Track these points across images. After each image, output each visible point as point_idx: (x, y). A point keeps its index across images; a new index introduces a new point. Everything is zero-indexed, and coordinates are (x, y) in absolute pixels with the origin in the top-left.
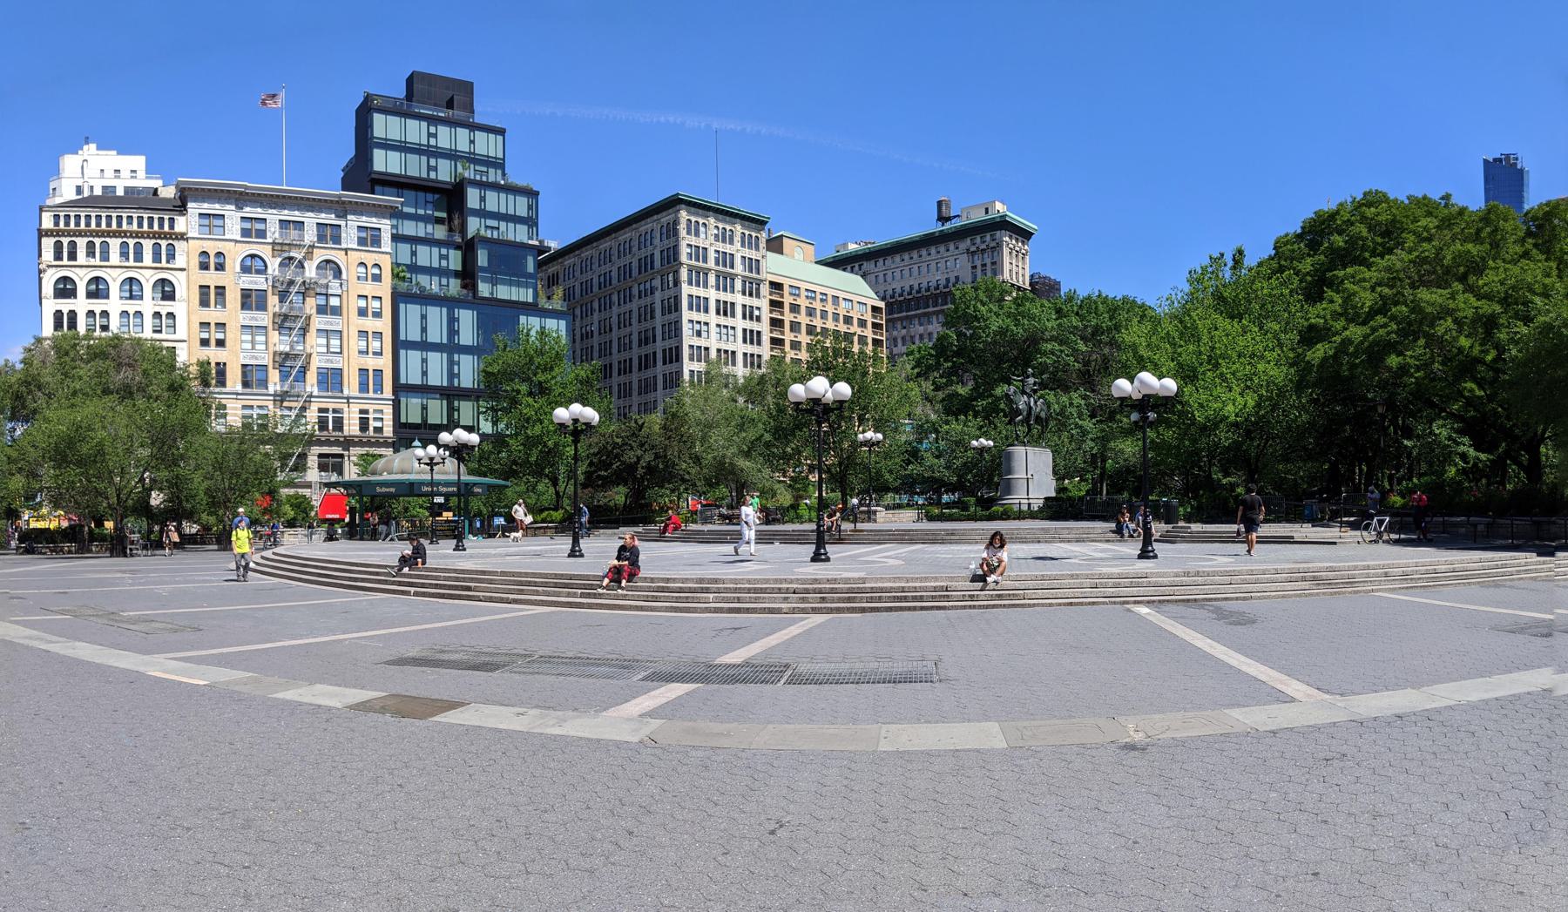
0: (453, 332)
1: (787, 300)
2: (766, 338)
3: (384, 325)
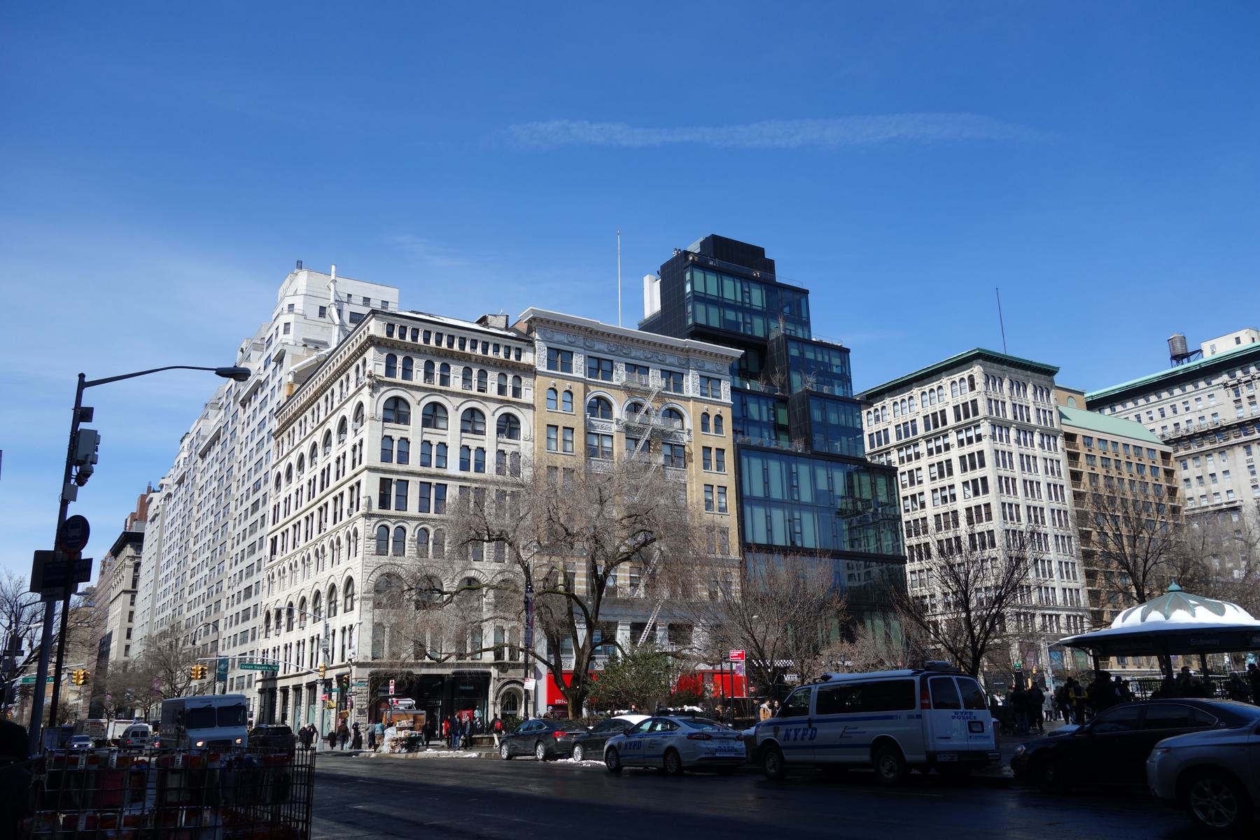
0: (792, 487)
1: (1083, 451)
2: (1068, 493)
3: (727, 478)
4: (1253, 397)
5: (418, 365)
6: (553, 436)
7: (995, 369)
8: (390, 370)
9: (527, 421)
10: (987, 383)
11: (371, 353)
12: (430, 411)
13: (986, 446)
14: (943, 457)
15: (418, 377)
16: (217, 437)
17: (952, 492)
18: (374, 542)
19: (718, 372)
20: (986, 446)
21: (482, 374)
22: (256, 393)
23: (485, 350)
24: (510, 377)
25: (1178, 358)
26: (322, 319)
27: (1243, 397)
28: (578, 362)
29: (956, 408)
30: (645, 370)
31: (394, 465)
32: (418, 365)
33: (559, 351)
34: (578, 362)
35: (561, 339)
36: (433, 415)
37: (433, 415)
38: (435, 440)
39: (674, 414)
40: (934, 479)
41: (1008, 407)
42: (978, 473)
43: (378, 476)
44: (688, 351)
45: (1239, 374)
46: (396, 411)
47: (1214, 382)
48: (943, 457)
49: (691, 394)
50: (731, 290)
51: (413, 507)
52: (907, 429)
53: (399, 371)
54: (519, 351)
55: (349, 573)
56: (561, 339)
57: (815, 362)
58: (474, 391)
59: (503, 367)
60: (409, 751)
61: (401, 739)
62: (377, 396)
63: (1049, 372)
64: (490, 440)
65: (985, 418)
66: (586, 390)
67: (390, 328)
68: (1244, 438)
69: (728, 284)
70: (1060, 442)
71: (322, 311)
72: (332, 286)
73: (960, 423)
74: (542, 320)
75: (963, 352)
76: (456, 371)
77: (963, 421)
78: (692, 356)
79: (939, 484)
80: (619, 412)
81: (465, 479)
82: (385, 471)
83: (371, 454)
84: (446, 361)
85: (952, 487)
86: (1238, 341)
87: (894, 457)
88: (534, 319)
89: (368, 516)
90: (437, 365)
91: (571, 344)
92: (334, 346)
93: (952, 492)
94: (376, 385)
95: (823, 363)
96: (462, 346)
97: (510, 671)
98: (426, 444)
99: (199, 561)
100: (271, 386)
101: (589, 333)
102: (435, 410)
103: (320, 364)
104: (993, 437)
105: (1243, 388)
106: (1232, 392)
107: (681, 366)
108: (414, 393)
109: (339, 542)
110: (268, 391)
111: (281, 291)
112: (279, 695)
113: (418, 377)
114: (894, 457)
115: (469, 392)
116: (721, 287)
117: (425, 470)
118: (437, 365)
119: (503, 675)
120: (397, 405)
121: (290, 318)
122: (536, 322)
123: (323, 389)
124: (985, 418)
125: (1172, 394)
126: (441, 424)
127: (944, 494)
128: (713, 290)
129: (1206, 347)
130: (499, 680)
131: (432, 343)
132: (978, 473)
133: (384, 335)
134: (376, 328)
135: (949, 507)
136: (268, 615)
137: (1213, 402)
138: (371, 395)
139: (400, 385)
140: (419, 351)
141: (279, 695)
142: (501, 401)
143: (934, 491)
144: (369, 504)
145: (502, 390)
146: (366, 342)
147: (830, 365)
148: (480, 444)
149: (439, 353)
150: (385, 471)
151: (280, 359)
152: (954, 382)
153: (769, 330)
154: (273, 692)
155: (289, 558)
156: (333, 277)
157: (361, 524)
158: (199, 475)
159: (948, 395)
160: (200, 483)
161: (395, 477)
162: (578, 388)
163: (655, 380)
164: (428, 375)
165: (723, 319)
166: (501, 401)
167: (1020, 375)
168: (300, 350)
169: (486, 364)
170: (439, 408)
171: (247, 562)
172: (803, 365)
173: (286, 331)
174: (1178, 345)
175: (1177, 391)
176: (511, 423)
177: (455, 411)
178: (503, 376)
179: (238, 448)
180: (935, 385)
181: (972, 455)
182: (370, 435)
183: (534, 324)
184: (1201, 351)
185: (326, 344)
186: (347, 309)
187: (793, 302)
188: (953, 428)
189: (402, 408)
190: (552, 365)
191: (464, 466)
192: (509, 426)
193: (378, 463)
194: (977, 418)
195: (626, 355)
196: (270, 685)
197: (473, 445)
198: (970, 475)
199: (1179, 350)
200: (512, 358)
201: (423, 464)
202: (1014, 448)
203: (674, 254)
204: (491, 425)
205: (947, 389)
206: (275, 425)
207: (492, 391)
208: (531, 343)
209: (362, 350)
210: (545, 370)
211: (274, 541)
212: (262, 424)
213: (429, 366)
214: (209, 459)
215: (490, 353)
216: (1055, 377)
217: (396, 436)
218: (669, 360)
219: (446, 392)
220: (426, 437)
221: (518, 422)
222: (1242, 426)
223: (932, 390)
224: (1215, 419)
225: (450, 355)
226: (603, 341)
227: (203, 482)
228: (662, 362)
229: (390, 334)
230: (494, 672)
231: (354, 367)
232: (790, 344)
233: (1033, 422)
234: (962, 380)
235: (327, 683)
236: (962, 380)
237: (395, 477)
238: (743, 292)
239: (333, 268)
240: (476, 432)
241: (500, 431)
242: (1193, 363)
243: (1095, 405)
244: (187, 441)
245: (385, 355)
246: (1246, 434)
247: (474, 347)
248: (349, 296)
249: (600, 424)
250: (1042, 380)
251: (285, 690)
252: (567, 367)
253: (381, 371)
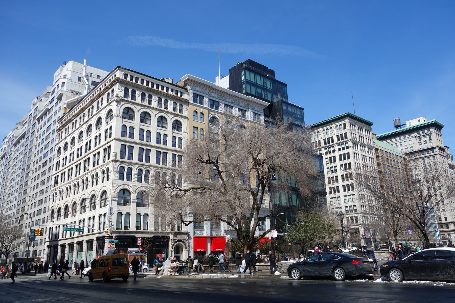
4: (426, 141)
5: (138, 94)
6: (196, 132)
7: (353, 121)
8: (126, 95)
9: (185, 123)
10: (350, 126)
11: (117, 87)
12: (143, 116)
13: (350, 150)
14: (332, 155)
15: (138, 99)
16: (23, 136)
17: (336, 168)
18: (118, 174)
19: (259, 111)
20: (350, 150)
21: (166, 102)
22: (42, 118)
23: (167, 91)
24: (178, 104)
25: (397, 127)
26: (79, 82)
27: (422, 141)
28: (206, 101)
29: (325, 140)
30: (232, 107)
31: (127, 138)
32: (138, 94)
33: (198, 95)
34: (206, 101)
35: (199, 90)
36: (145, 117)
37: (145, 117)
38: (146, 129)
40: (328, 163)
41: (357, 136)
42: (347, 161)
43: (120, 143)
44: (249, 101)
45: (421, 132)
46: (128, 113)
47: (411, 135)
48: (332, 155)
49: (249, 119)
50: (259, 81)
51: (136, 158)
52: (329, 141)
53: (130, 96)
54: (182, 93)
55: (104, 189)
56: (199, 90)
58: (163, 108)
59: (175, 99)
60: (180, 275)
61: (174, 268)
62: (120, 106)
63: (369, 124)
64: (169, 131)
65: (350, 140)
66: (209, 113)
67: (126, 76)
68: (422, 156)
69: (258, 78)
70: (374, 151)
71: (79, 79)
72: (84, 68)
73: (326, 145)
74: (191, 80)
75: (342, 114)
76: (155, 99)
77: (327, 145)
78: (250, 103)
79: (330, 165)
81: (159, 148)
82: (123, 141)
83: (116, 132)
84: (151, 94)
85: (335, 167)
86: (419, 121)
87: (323, 151)
88: (188, 79)
89: (115, 161)
90: (147, 95)
91: (203, 92)
92: (86, 94)
93: (336, 168)
94: (119, 101)
95: (294, 113)
96: (158, 87)
97: (178, 236)
98: (142, 130)
99: (13, 190)
100: (54, 110)
102: (145, 115)
103: (79, 102)
104: (353, 147)
105: (422, 138)
106: (418, 139)
107: (245, 107)
108: (136, 106)
109: (70, 188)
110: (52, 112)
111: (56, 74)
112: (60, 249)
113: (138, 99)
114: (323, 151)
115: (160, 108)
116: (256, 79)
117: (141, 142)
118: (147, 95)
119: (175, 238)
120: (128, 111)
121: (65, 80)
123: (87, 106)
124: (350, 140)
125: (396, 139)
126: (148, 122)
127: (332, 169)
128: (253, 80)
129: (407, 123)
130: (173, 240)
131: (145, 84)
132: (347, 161)
133: (123, 78)
134: (119, 74)
135: (334, 174)
136: (53, 211)
137: (411, 143)
138: (117, 105)
139: (130, 102)
140: (139, 87)
141: (60, 249)
142: (174, 114)
143: (328, 168)
144: (116, 156)
145: (174, 109)
146: (115, 81)
148: (165, 133)
150: (123, 141)
151: (60, 98)
152: (324, 130)
153: (273, 99)
154: (56, 247)
155: (66, 184)
156: (85, 64)
157: (111, 166)
158: (13, 154)
159: (335, 131)
160: (13, 156)
161: (128, 144)
162: (206, 112)
163: (235, 112)
164: (143, 99)
166: (174, 114)
167: (361, 124)
168: (70, 94)
169: (168, 97)
170: (147, 115)
171: (40, 189)
174: (397, 122)
175: (398, 138)
176: (178, 124)
178: (175, 103)
179: (35, 139)
180: (329, 127)
181: (344, 154)
182: (116, 124)
183: (188, 82)
184: (406, 124)
185: (81, 93)
187: (280, 88)
188: (323, 147)
189: (131, 113)
190: (195, 101)
191: (158, 142)
192: (177, 125)
193: (120, 137)
194: (347, 140)
195: (225, 100)
196: (54, 243)
197: (162, 133)
198: (343, 162)
199: (398, 124)
200: (179, 95)
201: (140, 139)
202: (359, 152)
203: (236, 64)
204: (170, 124)
205: (334, 129)
206: (57, 126)
207: (170, 109)
208: (187, 90)
209: (112, 85)
210: (192, 102)
211: (57, 178)
212: (49, 127)
213: (143, 95)
214: (18, 146)
215: (170, 92)
216: (372, 127)
217: (128, 125)
219: (151, 108)
220: (142, 127)
221: (181, 124)
222: (421, 151)
223: (327, 129)
224: (412, 149)
225: (151, 91)
226: (215, 93)
227: (15, 156)
228: (238, 105)
229: (126, 78)
230: (171, 236)
231: (106, 94)
233: (365, 143)
234: (340, 125)
235: (90, 242)
236: (340, 125)
237: (128, 144)
238: (264, 82)
239: (85, 61)
240: (163, 127)
241: (174, 128)
242: (403, 128)
243: (381, 139)
244: (7, 140)
245: (124, 88)
246: (428, 153)
247: (163, 88)
248: (91, 74)
250: (365, 127)
251: (63, 246)
252: (201, 103)
253: (122, 94)
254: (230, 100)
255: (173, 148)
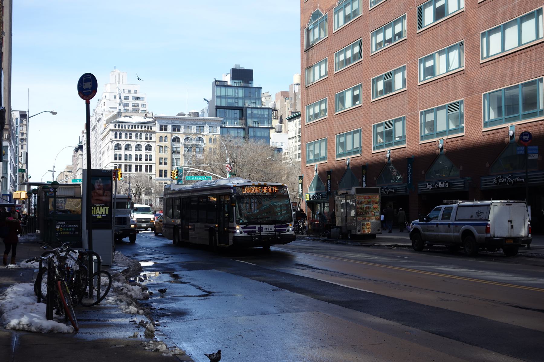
8: (116, 137)
9: (153, 145)
21: (141, 135)
23: (142, 128)
24: (149, 134)
28: (169, 128)
32: (123, 134)
35: (164, 122)
37: (127, 147)
39: (200, 139)
46: (118, 147)
57: (258, 114)
66: (172, 135)
71: (115, 97)
76: (133, 135)
80: (182, 140)
94: (112, 141)
95: (261, 114)
96: (135, 128)
98: (126, 155)
101: (172, 119)
116: (227, 92)
122: (157, 118)
126: (130, 149)
128: (223, 93)
133: (114, 128)
140: (123, 131)
145: (146, 138)
147: (264, 115)
149: (128, 131)
162: (169, 136)
163: (194, 130)
165: (227, 103)
168: (108, 113)
172: (253, 116)
173: (104, 105)
177: (133, 145)
185: (116, 108)
186: (123, 96)
189: (119, 146)
190: (161, 130)
191: (136, 159)
192: (149, 148)
195: (185, 124)
200: (150, 129)
204: (143, 148)
207: (144, 139)
208: (155, 124)
213: (126, 134)
218: (199, 123)
225: (132, 131)
229: (115, 127)
232: (247, 109)
238: (235, 92)
240: (139, 150)
241: (146, 149)
247: (138, 127)
249: (176, 144)
252: (166, 130)
253: (113, 137)
254: (189, 123)
255: (146, 162)
